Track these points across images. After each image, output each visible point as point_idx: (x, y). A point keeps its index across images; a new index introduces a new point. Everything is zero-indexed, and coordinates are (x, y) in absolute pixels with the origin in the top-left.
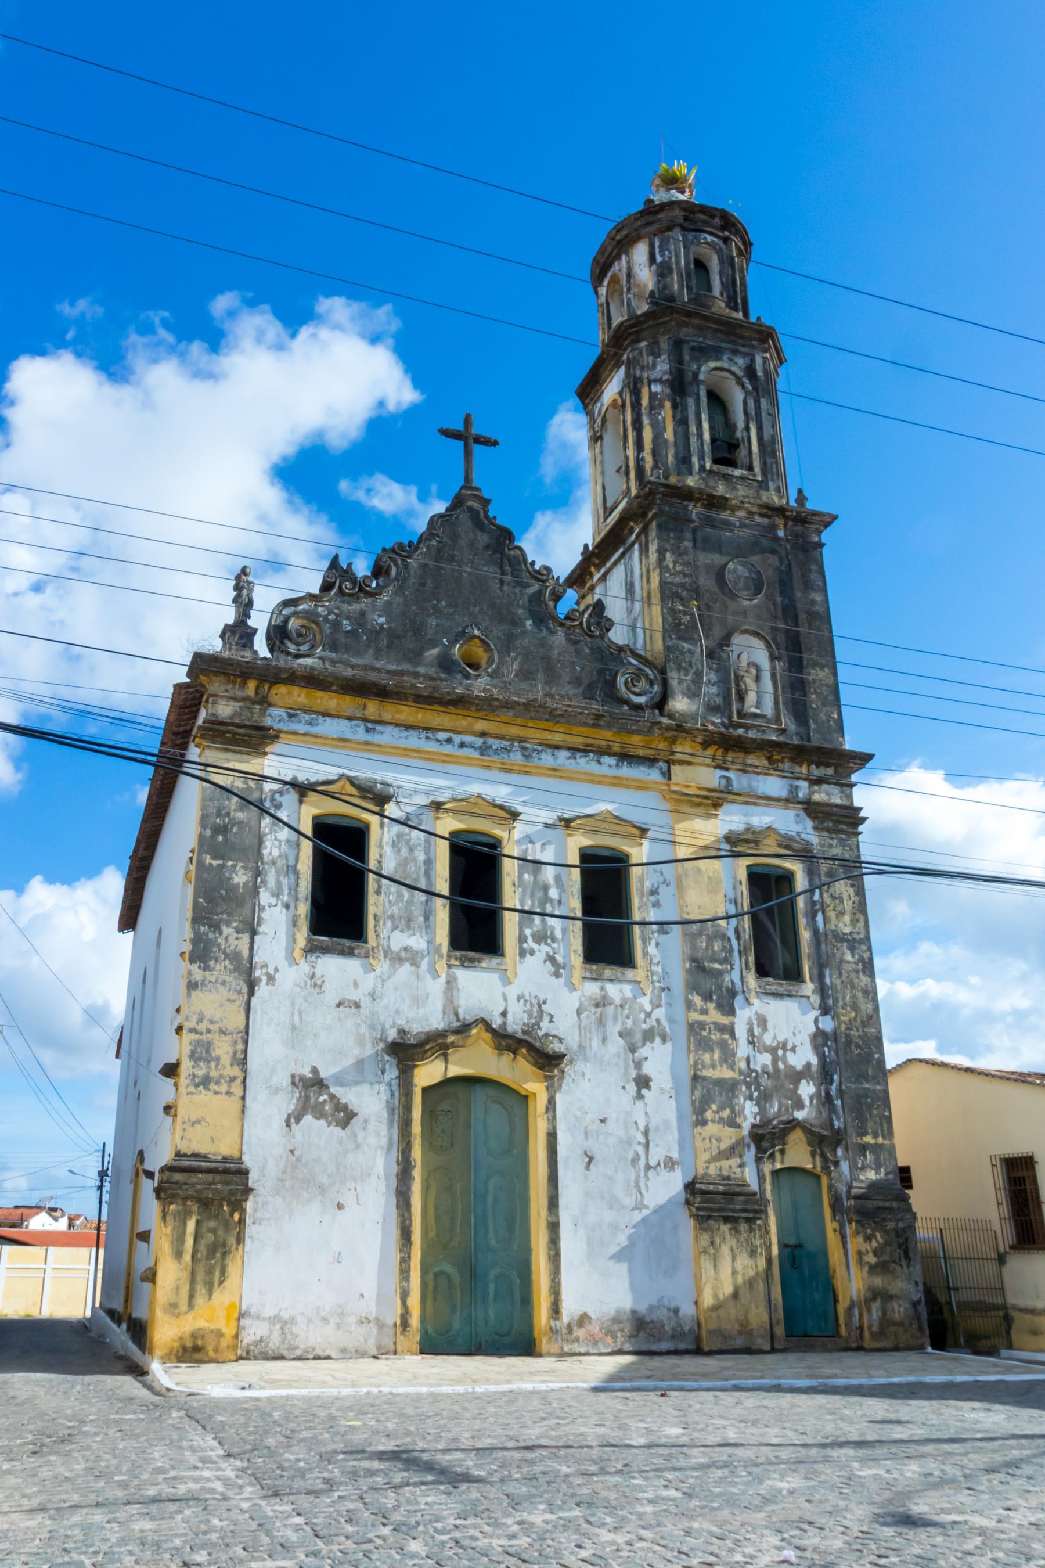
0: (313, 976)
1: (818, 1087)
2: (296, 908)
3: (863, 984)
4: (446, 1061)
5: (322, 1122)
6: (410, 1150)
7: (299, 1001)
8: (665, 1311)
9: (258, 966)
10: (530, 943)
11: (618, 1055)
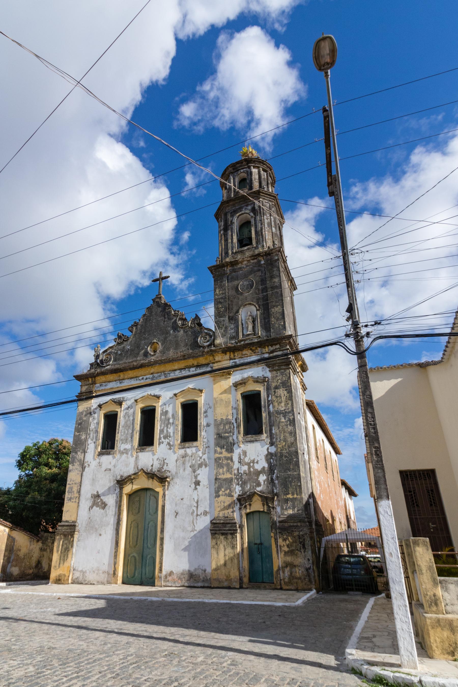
4: (133, 484)
10: (162, 439)
11: (189, 474)
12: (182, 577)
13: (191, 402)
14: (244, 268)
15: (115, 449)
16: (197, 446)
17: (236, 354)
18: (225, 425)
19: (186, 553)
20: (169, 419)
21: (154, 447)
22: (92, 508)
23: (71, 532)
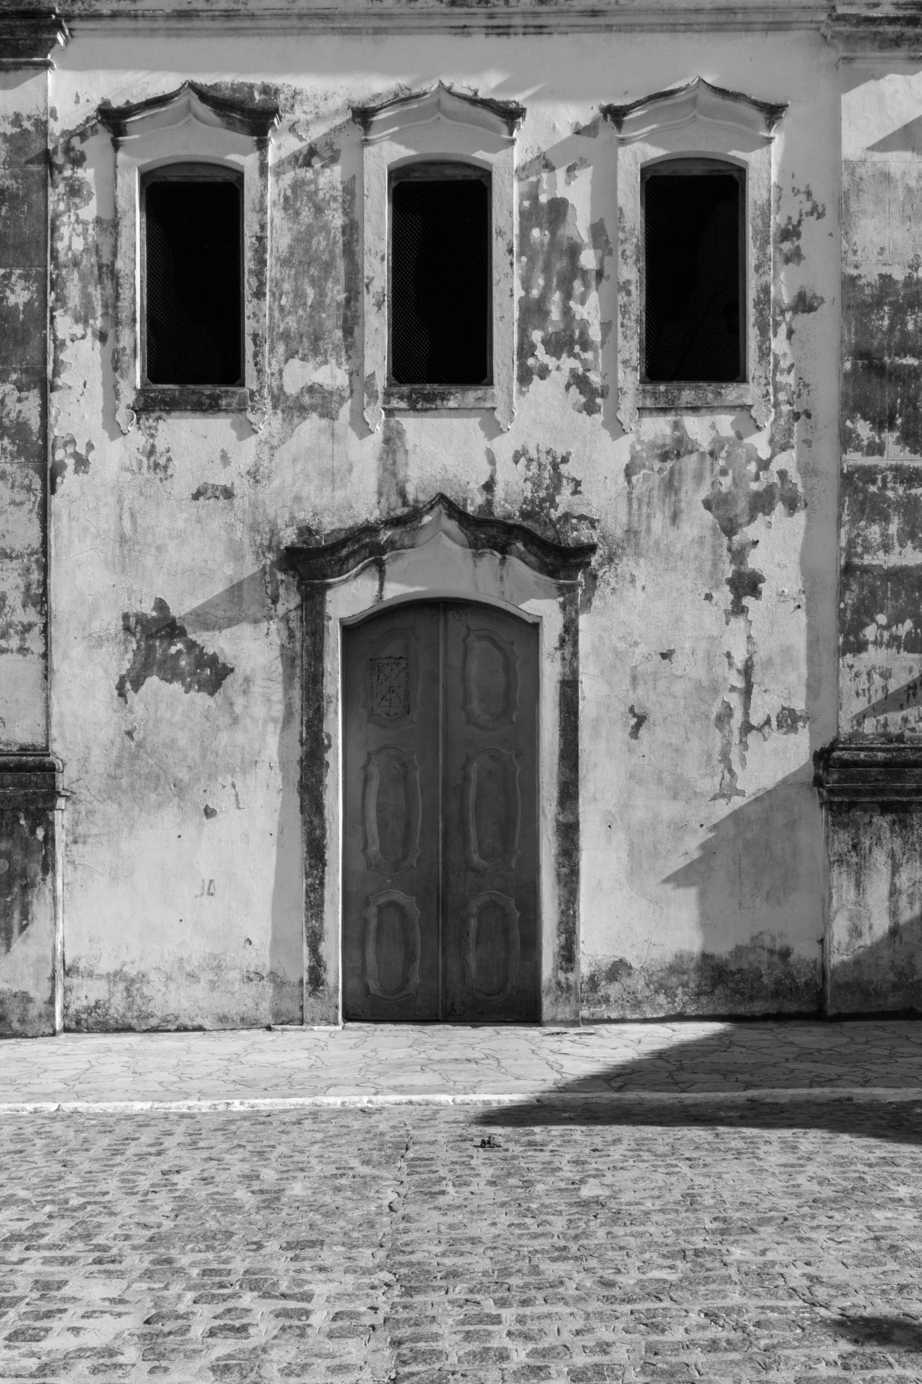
0: (152, 452)
2: (117, 339)
5: (177, 686)
6: (321, 721)
7: (129, 494)
8: (766, 955)
9: (60, 442)
11: (701, 541)
13: (698, 170)
15: (251, 383)
18: (899, 312)
20: (574, 251)
23: (28, 799)
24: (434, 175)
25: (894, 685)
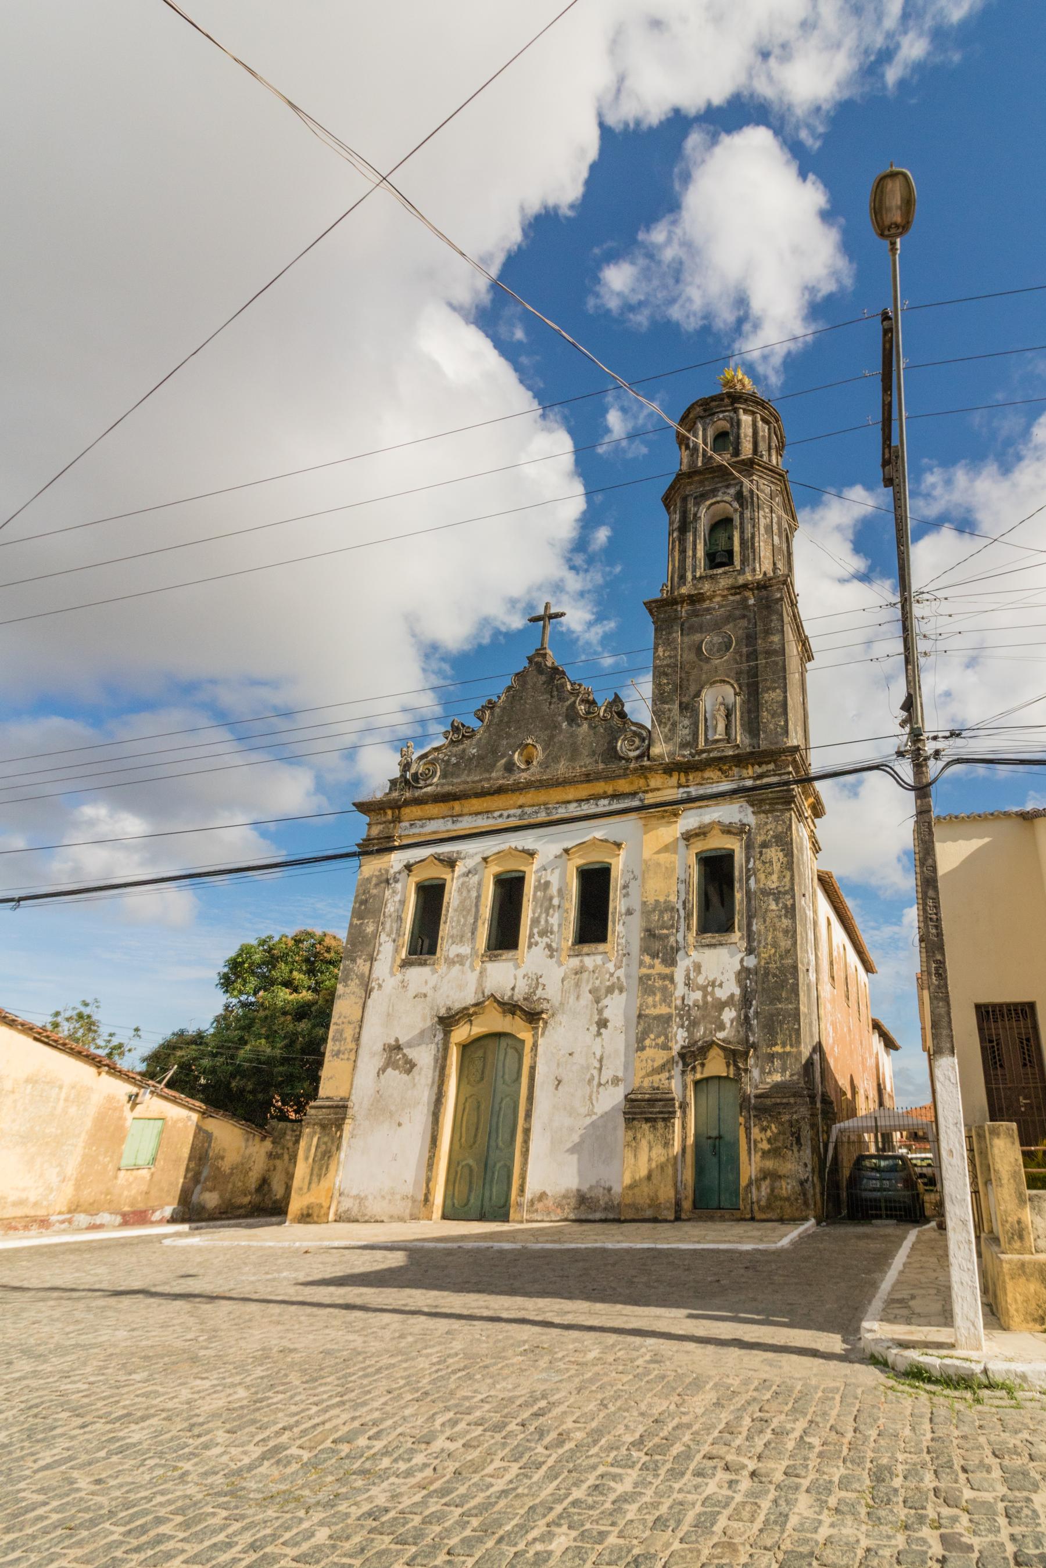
1: (739, 1012)
3: (784, 926)
12: (564, 1202)
13: (597, 866)
14: (714, 609)
16: (606, 953)
17: (691, 777)
18: (661, 913)
19: (575, 1157)
21: (519, 951)
22: (384, 1071)
24: (509, 876)
25: (656, 1065)
